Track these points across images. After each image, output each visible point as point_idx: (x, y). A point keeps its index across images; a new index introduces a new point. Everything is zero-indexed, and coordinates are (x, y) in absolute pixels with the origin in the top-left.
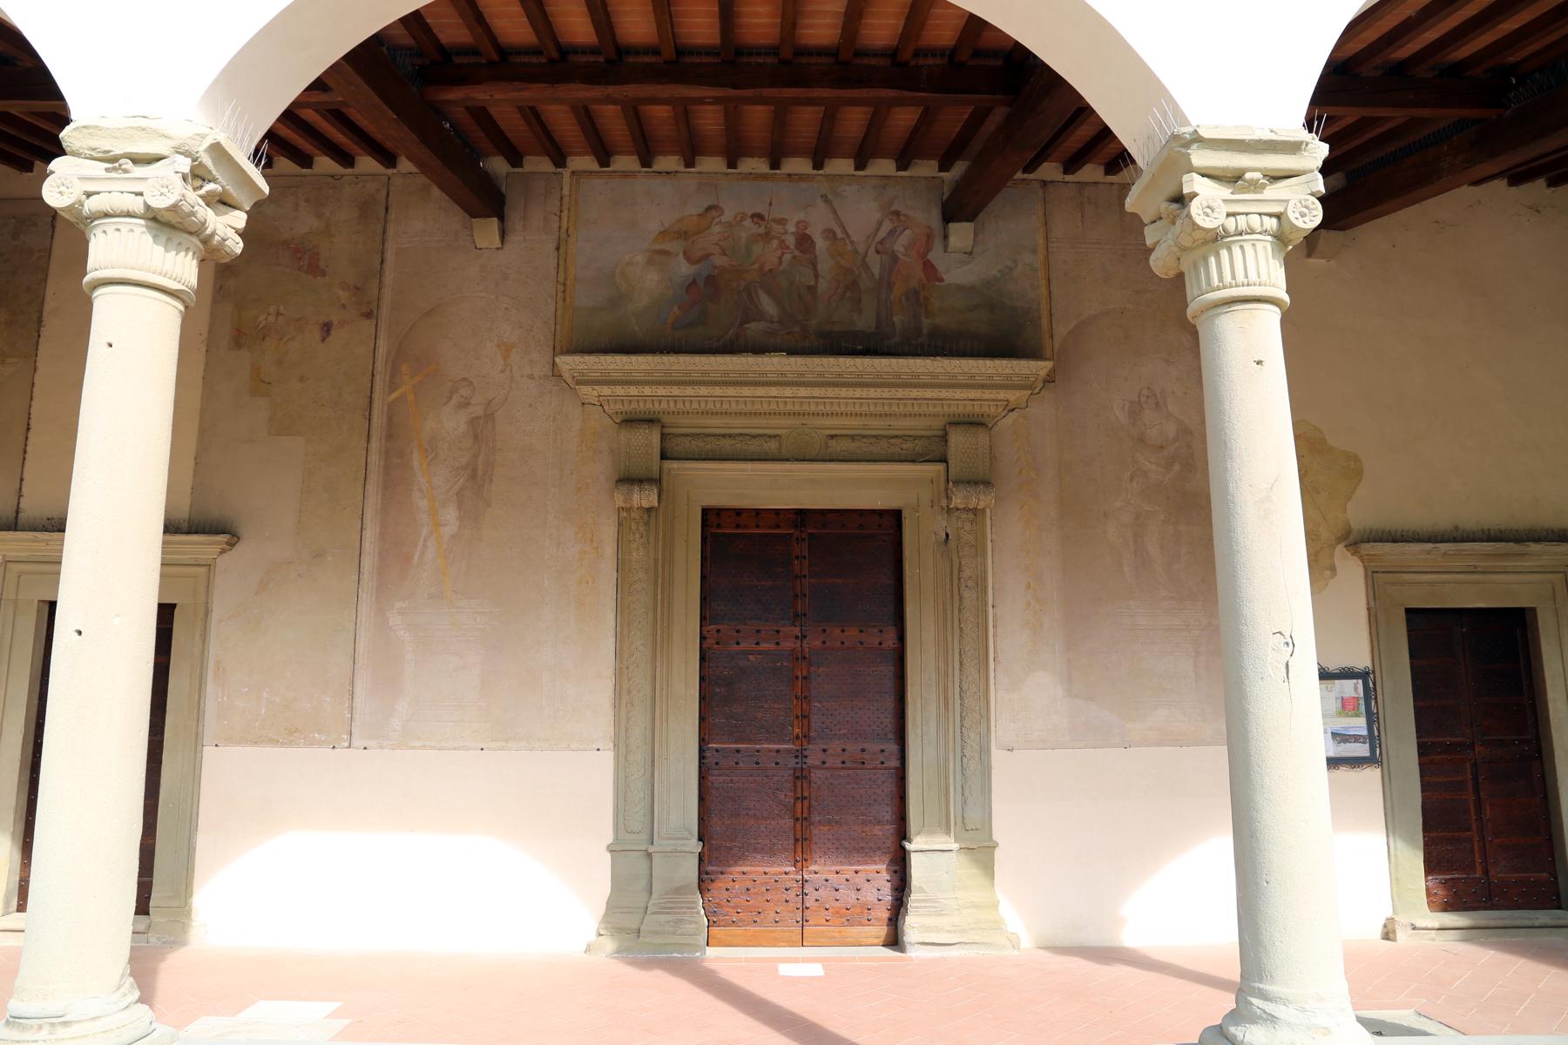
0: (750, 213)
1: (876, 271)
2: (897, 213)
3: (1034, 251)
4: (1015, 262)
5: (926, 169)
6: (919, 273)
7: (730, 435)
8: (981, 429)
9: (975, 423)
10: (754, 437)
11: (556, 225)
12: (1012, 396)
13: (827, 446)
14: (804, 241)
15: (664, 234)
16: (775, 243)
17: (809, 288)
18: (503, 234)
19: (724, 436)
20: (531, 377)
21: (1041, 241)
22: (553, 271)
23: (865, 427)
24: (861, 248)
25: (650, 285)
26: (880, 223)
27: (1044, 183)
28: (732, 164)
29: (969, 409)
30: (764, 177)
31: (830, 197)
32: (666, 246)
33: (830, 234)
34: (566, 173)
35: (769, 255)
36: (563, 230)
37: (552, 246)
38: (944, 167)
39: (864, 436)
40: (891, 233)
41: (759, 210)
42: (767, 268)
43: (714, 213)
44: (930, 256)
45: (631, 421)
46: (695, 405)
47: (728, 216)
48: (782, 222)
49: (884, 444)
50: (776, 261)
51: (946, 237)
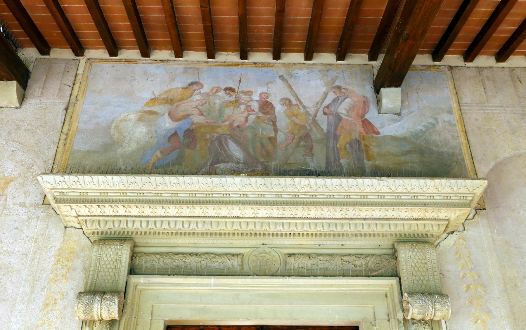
0: (223, 87)
1: (324, 127)
2: (339, 88)
3: (450, 112)
4: (436, 119)
5: (359, 59)
6: (359, 128)
7: (196, 254)
8: (427, 246)
9: (420, 240)
11: (68, 93)
12: (454, 215)
13: (286, 263)
14: (266, 106)
15: (154, 101)
16: (243, 107)
17: (270, 139)
18: (22, 99)
19: (191, 254)
20: (23, 205)
21: (455, 105)
22: (60, 125)
23: (320, 246)
24: (312, 111)
26: (326, 95)
27: (451, 68)
28: (211, 56)
29: (414, 228)
30: (236, 64)
31: (286, 77)
33: (287, 102)
34: (82, 60)
35: (238, 116)
37: (63, 107)
38: (373, 57)
39: (320, 255)
40: (335, 101)
41: (231, 85)
42: (235, 124)
43: (195, 87)
46: (165, 226)
47: (206, 89)
48: (249, 93)
49: (338, 261)
50: (243, 119)
51: (379, 102)
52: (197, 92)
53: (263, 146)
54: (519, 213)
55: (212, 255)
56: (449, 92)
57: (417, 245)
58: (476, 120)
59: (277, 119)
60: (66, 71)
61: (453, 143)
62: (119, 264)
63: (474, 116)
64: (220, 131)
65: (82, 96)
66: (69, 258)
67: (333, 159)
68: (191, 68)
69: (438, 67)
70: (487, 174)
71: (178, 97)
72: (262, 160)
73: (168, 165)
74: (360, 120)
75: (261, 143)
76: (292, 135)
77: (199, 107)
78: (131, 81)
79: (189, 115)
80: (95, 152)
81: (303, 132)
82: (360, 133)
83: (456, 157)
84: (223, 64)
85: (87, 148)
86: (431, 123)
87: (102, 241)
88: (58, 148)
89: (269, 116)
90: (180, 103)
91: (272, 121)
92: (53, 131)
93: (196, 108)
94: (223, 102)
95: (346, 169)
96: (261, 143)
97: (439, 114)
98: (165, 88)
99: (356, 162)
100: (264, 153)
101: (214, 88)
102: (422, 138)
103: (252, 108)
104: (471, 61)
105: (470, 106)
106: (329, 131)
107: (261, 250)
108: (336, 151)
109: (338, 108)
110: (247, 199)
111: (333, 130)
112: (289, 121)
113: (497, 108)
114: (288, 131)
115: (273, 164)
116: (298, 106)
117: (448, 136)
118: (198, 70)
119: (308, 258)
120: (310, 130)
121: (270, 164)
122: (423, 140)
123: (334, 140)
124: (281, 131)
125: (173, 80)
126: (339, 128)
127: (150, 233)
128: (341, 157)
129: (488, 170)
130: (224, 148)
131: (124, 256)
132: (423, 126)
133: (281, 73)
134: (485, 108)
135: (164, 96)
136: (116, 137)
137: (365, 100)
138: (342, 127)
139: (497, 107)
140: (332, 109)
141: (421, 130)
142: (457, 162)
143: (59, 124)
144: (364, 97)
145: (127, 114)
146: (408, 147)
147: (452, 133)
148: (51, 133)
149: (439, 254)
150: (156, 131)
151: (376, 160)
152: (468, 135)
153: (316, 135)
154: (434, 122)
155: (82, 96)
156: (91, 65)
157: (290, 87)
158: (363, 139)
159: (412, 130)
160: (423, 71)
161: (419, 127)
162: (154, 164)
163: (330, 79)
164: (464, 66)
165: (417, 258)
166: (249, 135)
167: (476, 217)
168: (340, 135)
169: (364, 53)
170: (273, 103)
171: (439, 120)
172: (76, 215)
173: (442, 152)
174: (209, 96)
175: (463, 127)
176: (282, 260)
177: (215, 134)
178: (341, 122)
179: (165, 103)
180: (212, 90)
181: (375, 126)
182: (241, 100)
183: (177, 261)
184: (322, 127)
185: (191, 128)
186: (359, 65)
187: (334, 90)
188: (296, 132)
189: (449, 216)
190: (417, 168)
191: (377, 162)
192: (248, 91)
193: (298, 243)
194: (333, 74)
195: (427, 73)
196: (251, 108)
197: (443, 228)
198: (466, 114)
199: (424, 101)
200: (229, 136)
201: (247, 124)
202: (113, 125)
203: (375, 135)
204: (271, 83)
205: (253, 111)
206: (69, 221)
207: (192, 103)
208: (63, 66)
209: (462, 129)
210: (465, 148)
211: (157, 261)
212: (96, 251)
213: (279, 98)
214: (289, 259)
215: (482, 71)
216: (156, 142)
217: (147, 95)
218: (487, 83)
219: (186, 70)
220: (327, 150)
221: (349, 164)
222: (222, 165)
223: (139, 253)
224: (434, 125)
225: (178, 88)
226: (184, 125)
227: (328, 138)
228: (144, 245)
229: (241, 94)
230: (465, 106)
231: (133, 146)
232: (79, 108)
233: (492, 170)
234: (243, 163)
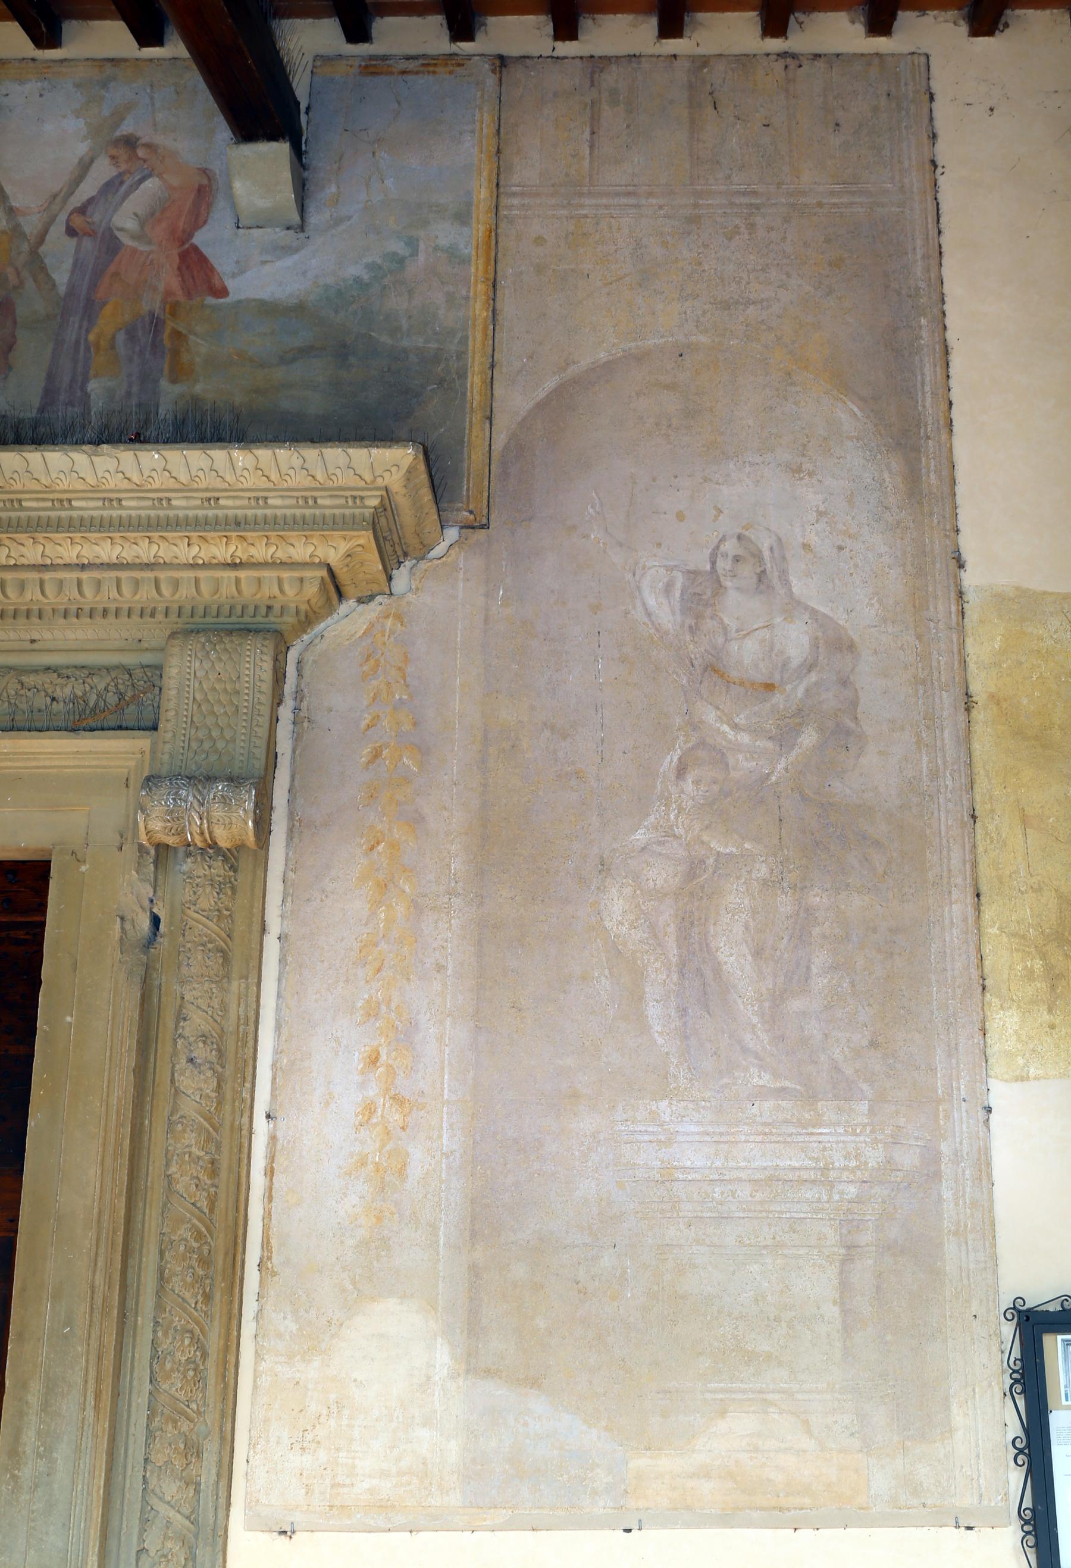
1: (62, 277)
2: (130, 142)
3: (462, 217)
4: (412, 243)
6: (168, 278)
21: (483, 194)
24: (30, 225)
27: (502, 62)
40: (109, 187)
44: (200, 239)
54: (586, 536)
58: (540, 241)
67: (67, 379)
70: (524, 419)
74: (175, 253)
83: (443, 365)
86: (395, 254)
99: (135, 389)
109: (115, 211)
111: (85, 288)
113: (616, 201)
120: (15, 288)
128: (92, 373)
129: (532, 404)
137: (205, 182)
138: (116, 274)
139: (617, 194)
140: (96, 216)
141: (357, 280)
142: (441, 382)
144: (204, 171)
147: (451, 288)
159: (330, 280)
160: (410, 78)
161: (354, 270)
163: (106, 112)
164: (549, 53)
168: (105, 304)
171: (422, 246)
175: (491, 268)
184: (55, 276)
187: (114, 152)
190: (315, 404)
191: (198, 388)
194: (119, 93)
195: (422, 81)
198: (511, 221)
199: (389, 183)
203: (211, 300)
209: (486, 272)
210: (479, 336)
218: (607, 112)
224: (401, 261)
230: (514, 194)
233: (540, 406)
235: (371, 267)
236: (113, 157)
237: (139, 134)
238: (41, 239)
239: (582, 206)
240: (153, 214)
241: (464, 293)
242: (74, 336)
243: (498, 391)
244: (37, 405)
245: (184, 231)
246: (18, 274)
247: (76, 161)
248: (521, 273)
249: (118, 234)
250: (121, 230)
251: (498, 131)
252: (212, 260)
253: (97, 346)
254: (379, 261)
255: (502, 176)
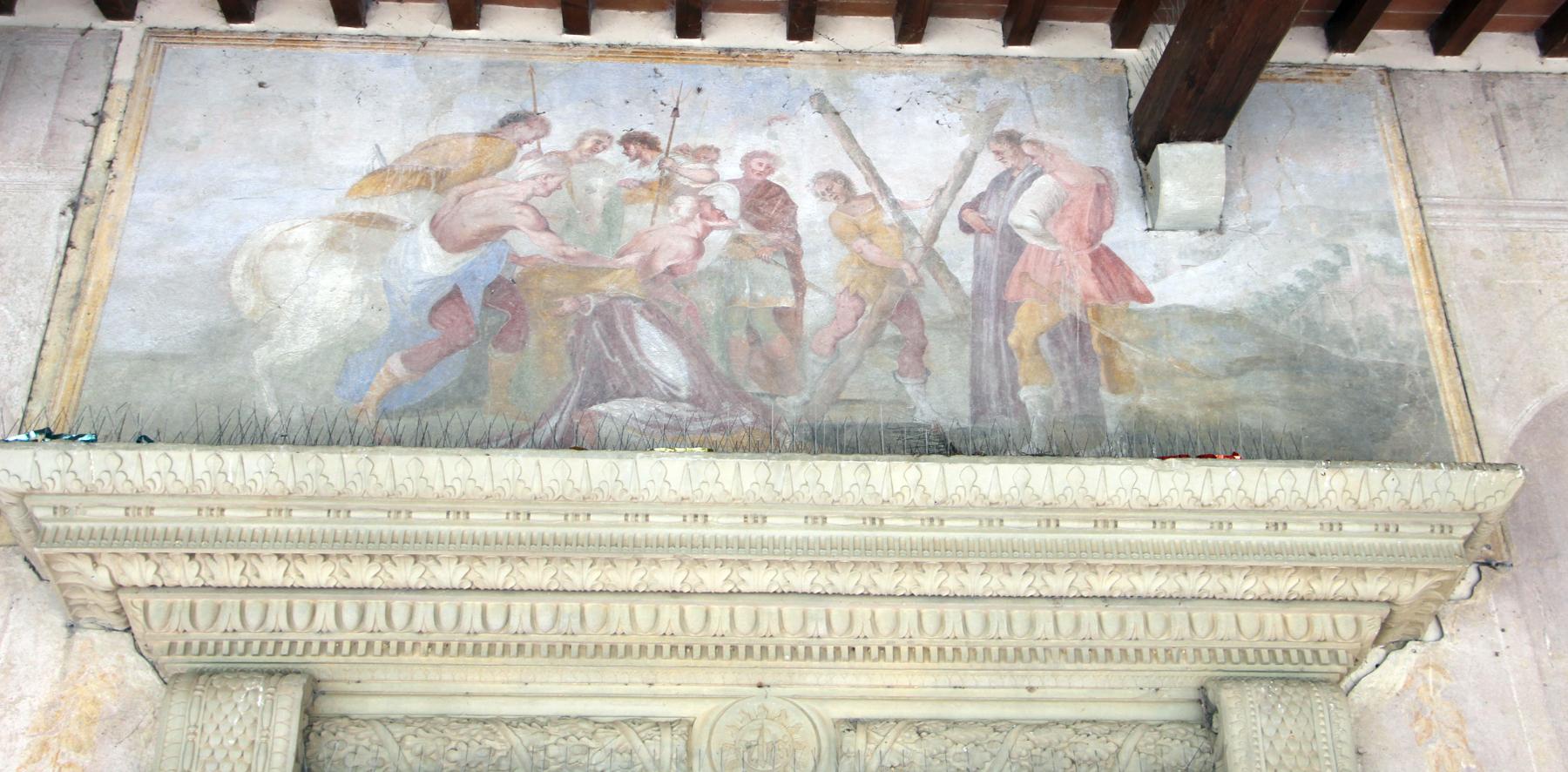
0: (618, 133)
2: (1013, 138)
3: (1389, 226)
4: (1340, 251)
5: (1080, 42)
6: (1083, 280)
7: (530, 721)
8: (1318, 695)
10: (612, 725)
11: (80, 150)
13: (839, 754)
14: (765, 200)
15: (379, 178)
16: (685, 204)
17: (779, 314)
22: (50, 264)
24: (921, 219)
25: (327, 303)
30: (664, 54)
31: (833, 100)
32: (386, 205)
33: (835, 186)
34: (131, 30)
35: (668, 232)
36: (98, 163)
37: (61, 199)
38: (1127, 35)
39: (952, 724)
40: (1000, 183)
41: (642, 127)
42: (661, 264)
43: (522, 130)
44: (1108, 239)
45: (207, 673)
50: (687, 246)
51: (1147, 188)
52: (527, 148)
53: (755, 339)
55: (585, 725)
56: (1384, 159)
57: (1283, 693)
58: (1476, 254)
59: (804, 245)
60: (71, 72)
61: (1400, 332)
62: (261, 759)
63: (1468, 238)
64: (608, 285)
65: (131, 161)
66: (83, 737)
67: (994, 386)
68: (507, 65)
69: (1346, 71)
70: (1516, 443)
71: (463, 166)
72: (753, 388)
73: (436, 403)
74: (1085, 254)
75: (750, 328)
76: (856, 303)
77: (534, 201)
78: (301, 108)
79: (503, 229)
80: (177, 358)
81: (890, 292)
82: (1087, 296)
84: (614, 50)
85: (147, 343)
86: (1325, 262)
87: (202, 678)
88: (44, 342)
89: (774, 236)
90: (470, 186)
91: (787, 254)
92: (26, 282)
93: (525, 204)
94: (619, 185)
95: (1042, 425)
96: (750, 328)
97: (1351, 231)
98: (419, 135)
100: (760, 364)
101: (587, 134)
102: (1294, 317)
103: (719, 205)
104: (1457, 50)
105: (1454, 206)
106: (979, 290)
107: (752, 706)
108: (1004, 357)
109: (1011, 205)
110: (709, 533)
111: (992, 287)
112: (842, 253)
113: (1546, 215)
114: (840, 287)
115: (791, 406)
116: (875, 200)
117: (1385, 311)
118: (531, 72)
119: (915, 737)
120: (914, 285)
121: (779, 402)
122: (1297, 323)
123: (996, 321)
124: (818, 289)
125: (446, 104)
126: (1014, 282)
127: (370, 645)
128: (1021, 379)
130: (622, 346)
131: (281, 730)
132: (1298, 274)
133: (815, 85)
134: (1504, 214)
135: (416, 163)
136: (250, 303)
137: (1103, 181)
138: (1025, 274)
139: (1547, 209)
141: (1291, 288)
143: (50, 259)
144: (1099, 170)
145: (286, 225)
146: (1245, 350)
147: (1395, 300)
148: (22, 289)
149: (1357, 720)
150: (386, 285)
151: (1141, 392)
152: (1448, 307)
153: (936, 303)
154: (1334, 260)
155: (131, 161)
156: (160, 52)
157: (847, 134)
158: (1098, 319)
159: (1262, 288)
161: (1287, 278)
162: (381, 399)
165: (1284, 735)
166: (708, 299)
167: (1480, 592)
168: (1018, 305)
169: (1097, 18)
170: (790, 191)
171: (1352, 255)
172: (108, 584)
173: (1362, 365)
174: (571, 162)
175: (1433, 279)
176: (824, 744)
177: (590, 297)
178: (1022, 257)
179: (419, 187)
180: (581, 141)
181: (1136, 271)
182: (680, 179)
183: (464, 747)
184: (957, 274)
185: (508, 277)
186: (1080, 60)
187: (998, 147)
188: (869, 289)
189: (1392, 592)
190: (1281, 421)
191: (1144, 400)
192: (706, 149)
193: (878, 680)
194: (992, 89)
195: (1311, 89)
196: (713, 208)
197: (1371, 631)
198: (1441, 232)
199: (1301, 188)
200: (639, 306)
201: (702, 264)
202: (239, 264)
203: (1135, 305)
204: (782, 119)
205: (722, 215)
206: (84, 606)
207: (513, 189)
208: (63, 51)
209: (1429, 285)
211: (394, 748)
212: (180, 711)
213: (809, 171)
214: (848, 737)
215: (1493, 85)
216: (386, 325)
217: (358, 159)
218: (1510, 125)
219: (489, 71)
220: (973, 354)
221: (1048, 403)
222: (617, 409)
223: (329, 718)
224: (1334, 270)
225: (462, 136)
226: (486, 264)
227: (977, 313)
228: (352, 687)
229: (680, 159)
230: (1438, 205)
231: (308, 339)
232: (116, 205)
233: (1530, 430)
234: (689, 400)
235: (1302, 274)
236: (997, 153)
237: (1020, 130)
238: (934, 234)
239: (1512, 219)
240: (1052, 212)
241: (1411, 306)
242: (991, 339)
243: (1478, 413)
244: (968, 413)
245: (1090, 231)
246: (915, 270)
247: (958, 155)
248: (1466, 287)
249: (1018, 231)
250: (1021, 227)
251: (1403, 141)
252: (1127, 262)
253: (1020, 349)
254: (1310, 269)
255: (1419, 188)
